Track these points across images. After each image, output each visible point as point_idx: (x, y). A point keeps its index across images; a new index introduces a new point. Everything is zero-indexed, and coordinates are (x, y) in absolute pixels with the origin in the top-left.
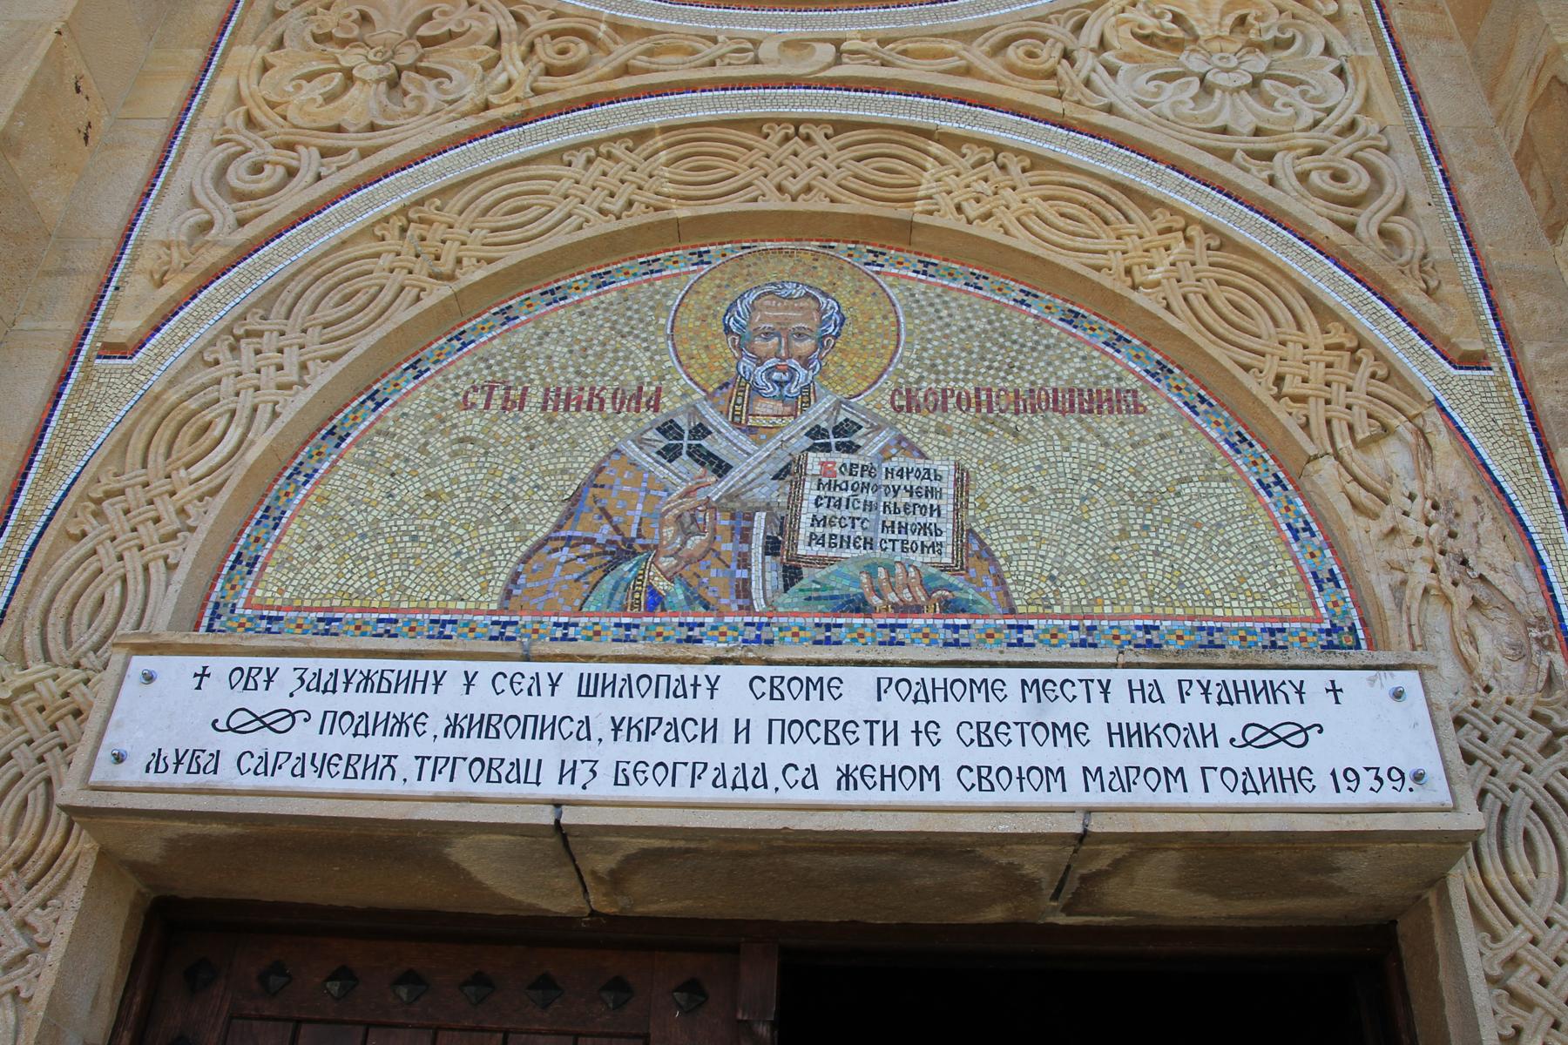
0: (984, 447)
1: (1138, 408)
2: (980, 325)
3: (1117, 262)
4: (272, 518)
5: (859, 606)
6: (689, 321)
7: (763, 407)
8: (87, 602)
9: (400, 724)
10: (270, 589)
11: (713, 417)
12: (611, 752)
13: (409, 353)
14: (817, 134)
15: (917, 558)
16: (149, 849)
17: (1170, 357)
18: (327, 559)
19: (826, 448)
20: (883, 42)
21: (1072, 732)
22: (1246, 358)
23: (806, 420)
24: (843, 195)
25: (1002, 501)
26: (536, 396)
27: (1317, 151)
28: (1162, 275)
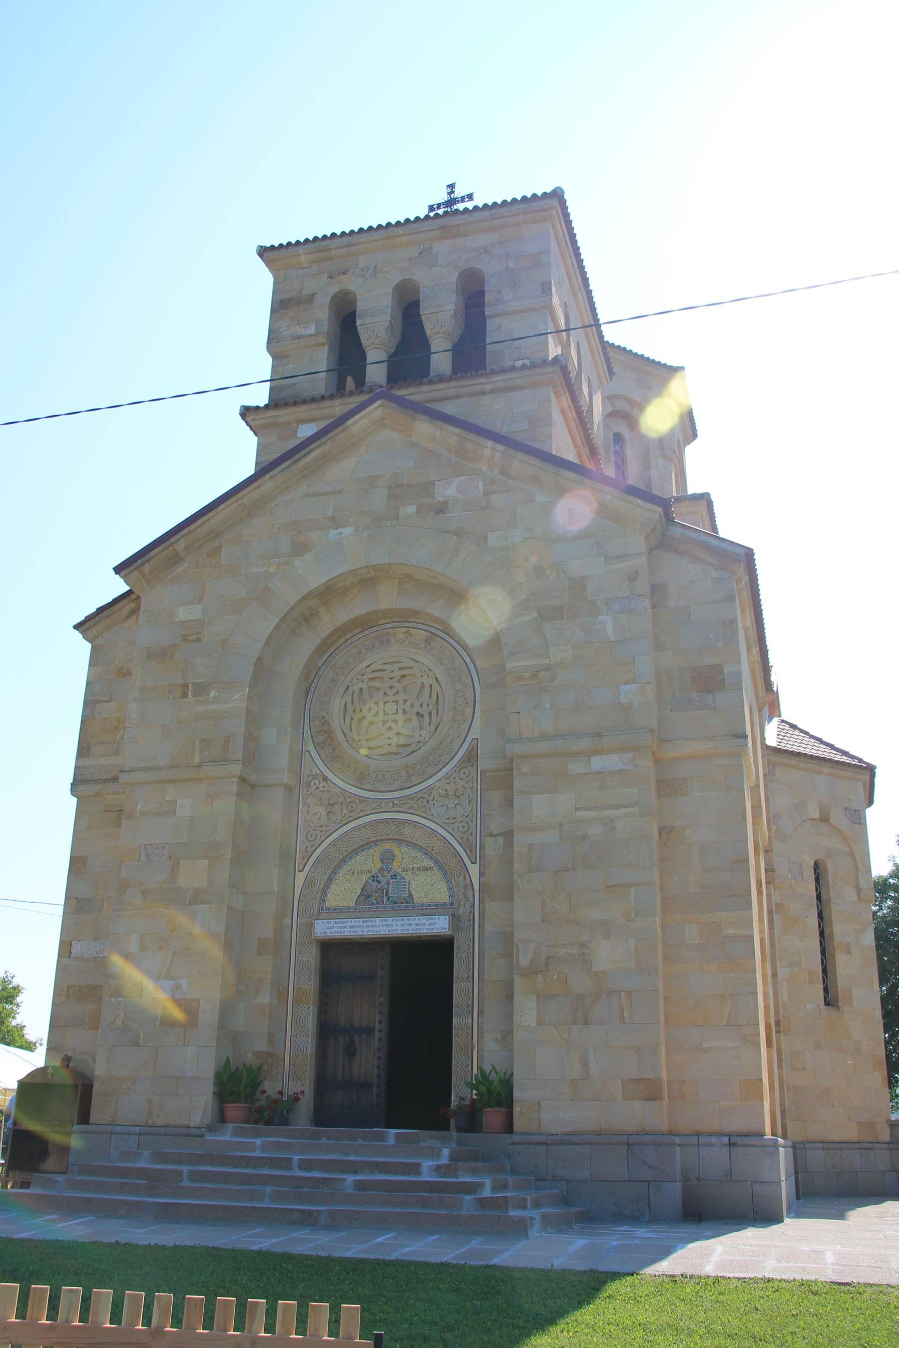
4: (326, 894)
5: (396, 903)
6: (375, 857)
9: (344, 927)
10: (328, 904)
12: (366, 929)
13: (339, 866)
21: (411, 925)
25: (414, 886)
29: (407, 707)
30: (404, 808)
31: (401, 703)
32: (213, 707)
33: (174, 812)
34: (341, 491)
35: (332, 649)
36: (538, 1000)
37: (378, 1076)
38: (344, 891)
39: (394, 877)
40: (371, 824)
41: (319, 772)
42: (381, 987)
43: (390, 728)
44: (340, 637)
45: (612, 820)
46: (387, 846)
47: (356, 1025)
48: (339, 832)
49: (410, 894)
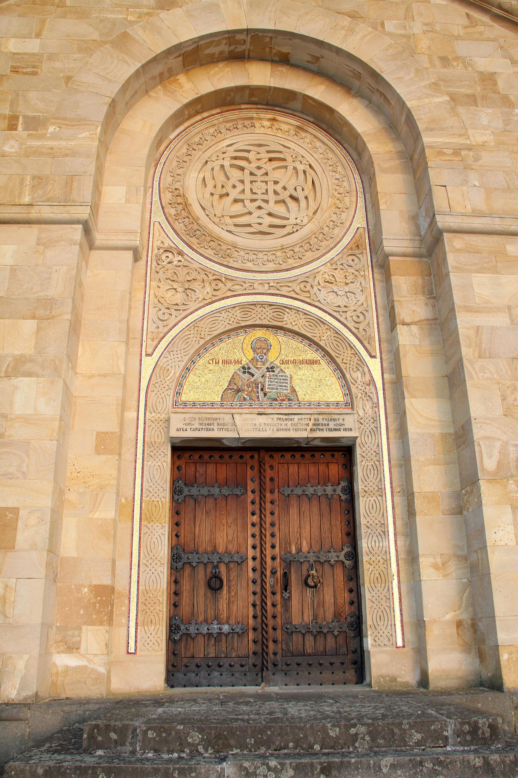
0: (295, 371)
1: (320, 364)
2: (294, 346)
3: (318, 335)
5: (276, 400)
6: (245, 346)
7: (259, 363)
8: (158, 402)
10: (184, 398)
11: (251, 366)
13: (198, 354)
14: (266, 306)
15: (284, 391)
16: (177, 441)
18: (192, 392)
19: (269, 371)
20: (277, 283)
22: (337, 355)
23: (266, 366)
24: (271, 320)
26: (221, 362)
27: (355, 311)
29: (278, 188)
31: (271, 184)
32: (50, 143)
35: (186, 125)
36: (514, 512)
37: (255, 617)
39: (271, 369)
40: (242, 306)
41: (173, 246)
42: (253, 503)
44: (197, 113)
46: (259, 333)
49: (294, 391)
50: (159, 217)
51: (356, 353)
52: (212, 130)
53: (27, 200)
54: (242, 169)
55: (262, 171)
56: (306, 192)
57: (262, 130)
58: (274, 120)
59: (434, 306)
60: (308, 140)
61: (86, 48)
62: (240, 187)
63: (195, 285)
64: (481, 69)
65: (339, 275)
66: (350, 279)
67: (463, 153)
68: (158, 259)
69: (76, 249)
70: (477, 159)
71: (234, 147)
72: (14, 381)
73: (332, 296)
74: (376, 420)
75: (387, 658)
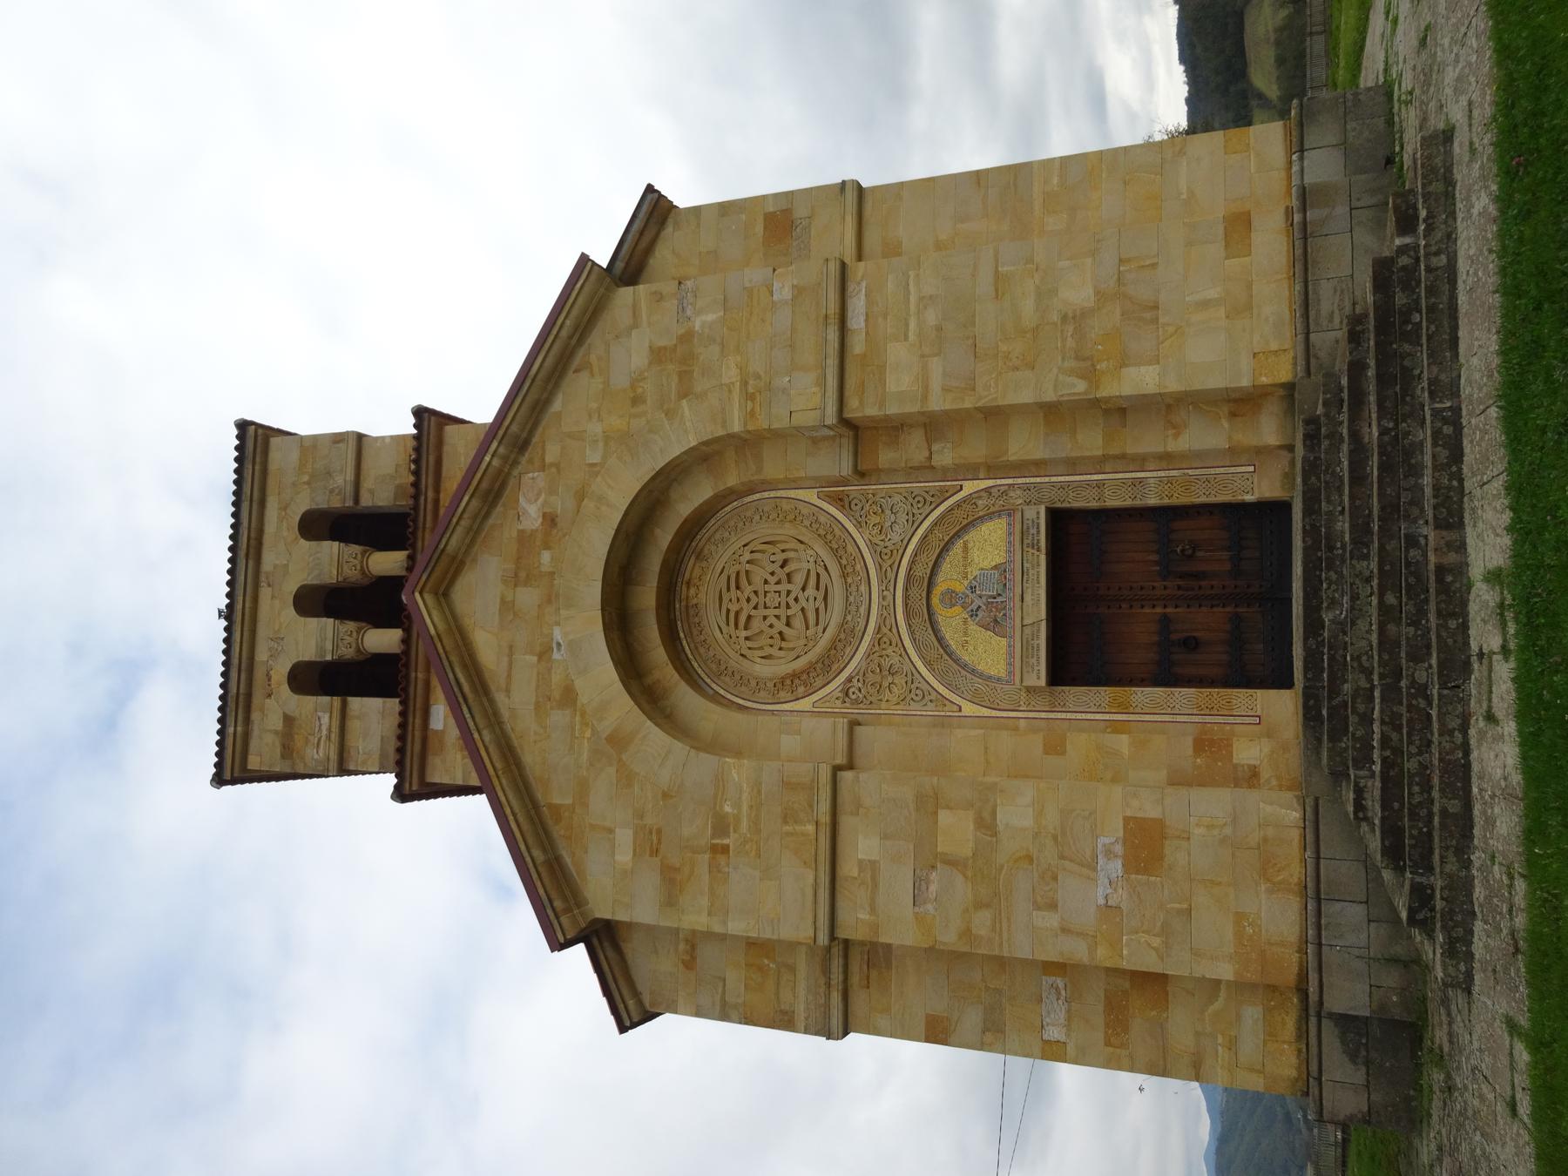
10: (1003, 674)
17: (957, 535)
28: (941, 535)
29: (772, 580)
30: (891, 575)
31: (767, 588)
32: (745, 808)
33: (873, 863)
34: (511, 647)
38: (988, 653)
39: (973, 589)
40: (908, 615)
43: (796, 600)
45: (921, 299)
46: (935, 601)
47: (1156, 638)
48: (915, 658)
49: (996, 567)
50: (805, 704)
51: (958, 505)
52: (702, 650)
53: (810, 828)
54: (749, 617)
55: (753, 596)
56: (777, 550)
57: (702, 596)
58: (688, 583)
59: (911, 426)
60: (713, 548)
61: (627, 778)
62: (773, 620)
63: (886, 664)
64: (646, 362)
65: (874, 519)
66: (877, 508)
67: (751, 390)
68: (857, 702)
69: (863, 776)
70: (758, 377)
71: (723, 625)
72: (1001, 827)
73: (896, 528)
74: (1027, 488)
75: (1261, 486)
